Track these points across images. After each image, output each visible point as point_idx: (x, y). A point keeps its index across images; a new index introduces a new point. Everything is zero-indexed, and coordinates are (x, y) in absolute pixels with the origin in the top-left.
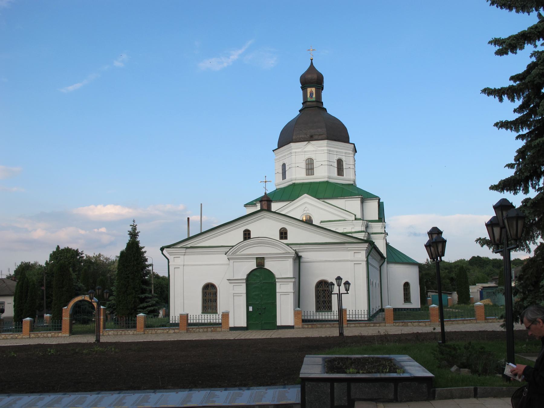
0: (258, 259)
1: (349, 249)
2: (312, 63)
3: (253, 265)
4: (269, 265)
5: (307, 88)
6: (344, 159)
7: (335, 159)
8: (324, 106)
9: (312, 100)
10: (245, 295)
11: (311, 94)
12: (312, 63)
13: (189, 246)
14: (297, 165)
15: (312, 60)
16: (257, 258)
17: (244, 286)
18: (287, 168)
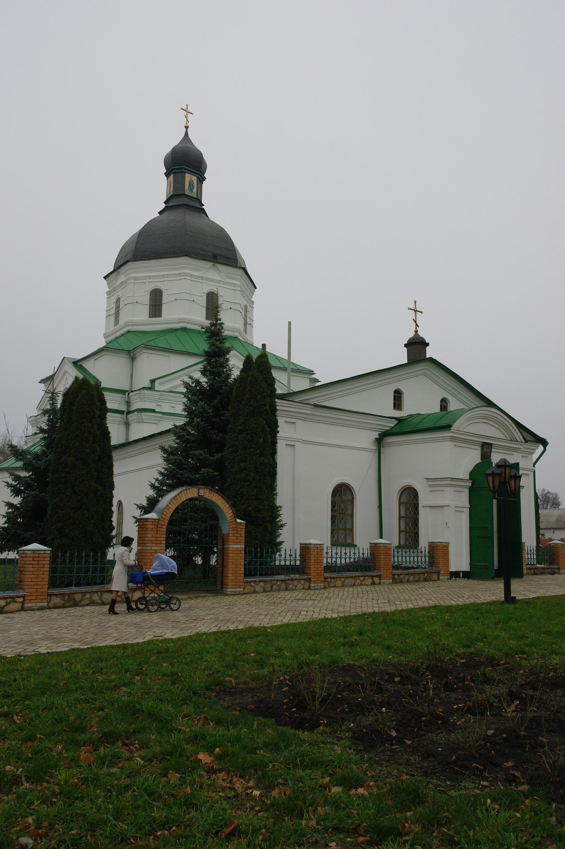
0: (485, 446)
2: (186, 134)
5: (185, 173)
9: (190, 195)
11: (191, 185)
12: (186, 134)
13: (312, 402)
15: (187, 128)
16: (484, 443)
17: (467, 492)
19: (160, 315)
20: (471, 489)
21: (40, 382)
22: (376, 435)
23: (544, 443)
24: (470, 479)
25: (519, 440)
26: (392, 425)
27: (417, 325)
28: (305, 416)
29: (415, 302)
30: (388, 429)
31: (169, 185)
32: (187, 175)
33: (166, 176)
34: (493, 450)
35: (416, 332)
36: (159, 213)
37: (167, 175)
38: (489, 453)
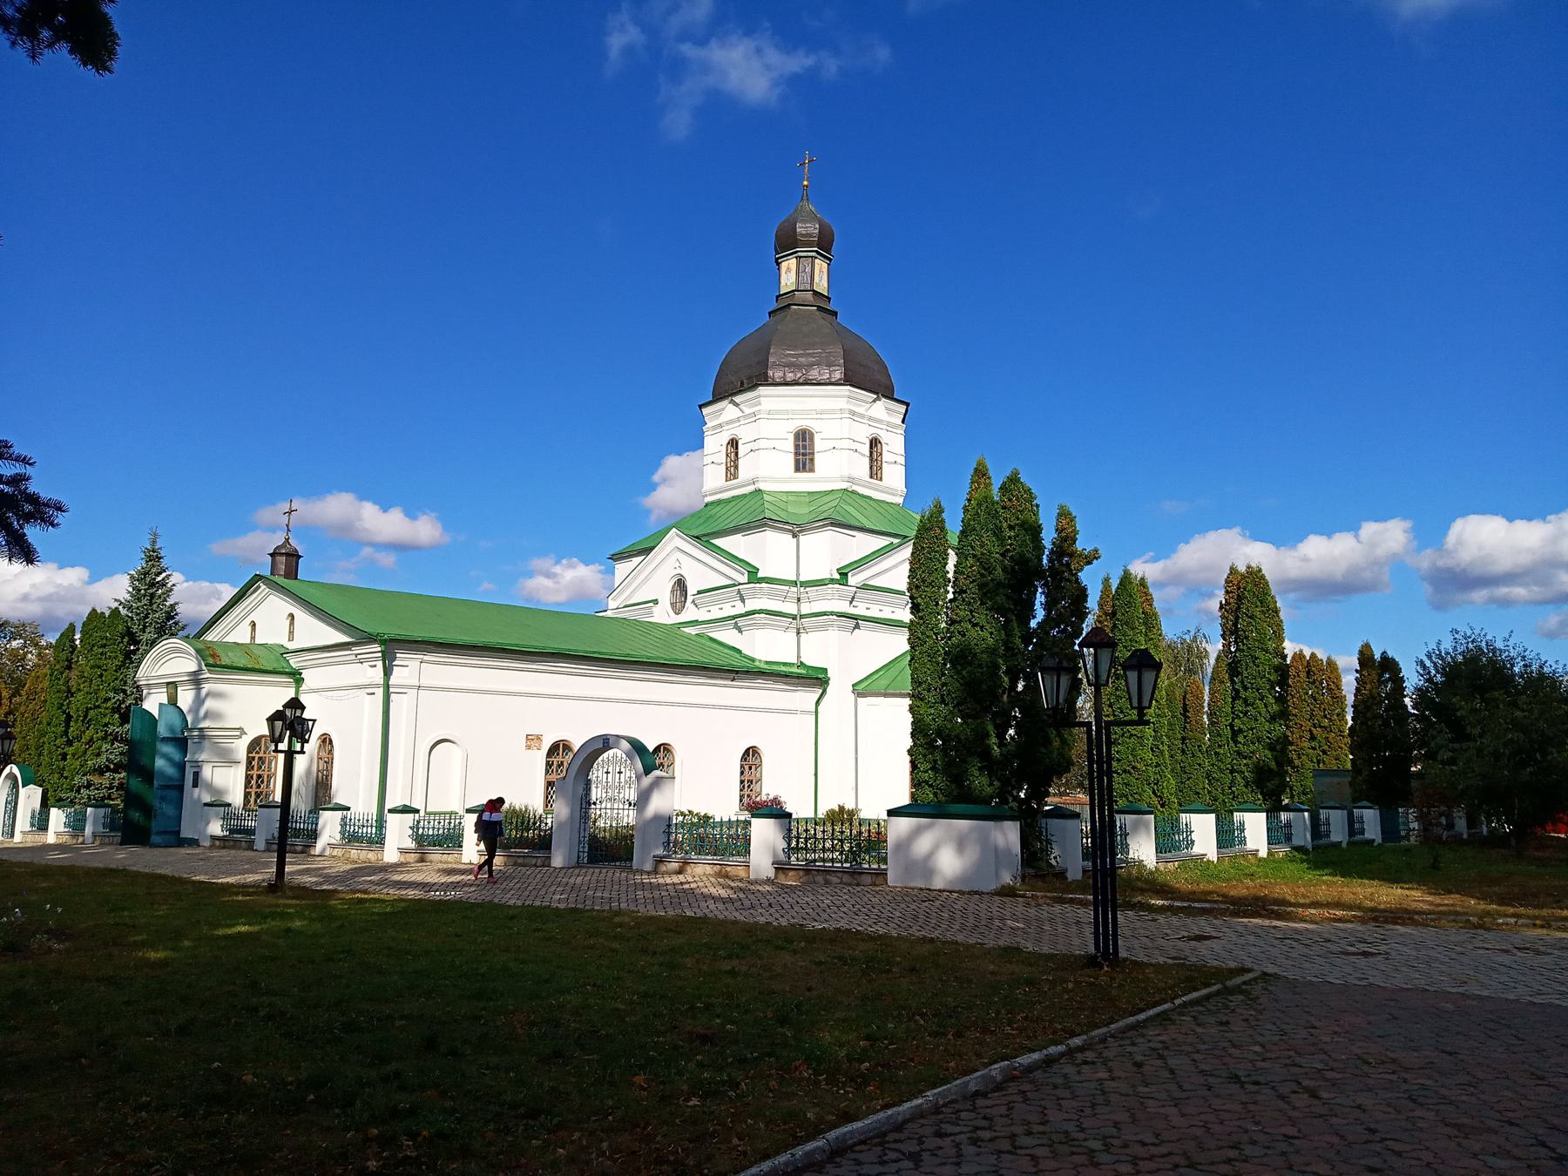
6: (884, 437)
7: (864, 433)
14: (771, 444)
18: (742, 450)
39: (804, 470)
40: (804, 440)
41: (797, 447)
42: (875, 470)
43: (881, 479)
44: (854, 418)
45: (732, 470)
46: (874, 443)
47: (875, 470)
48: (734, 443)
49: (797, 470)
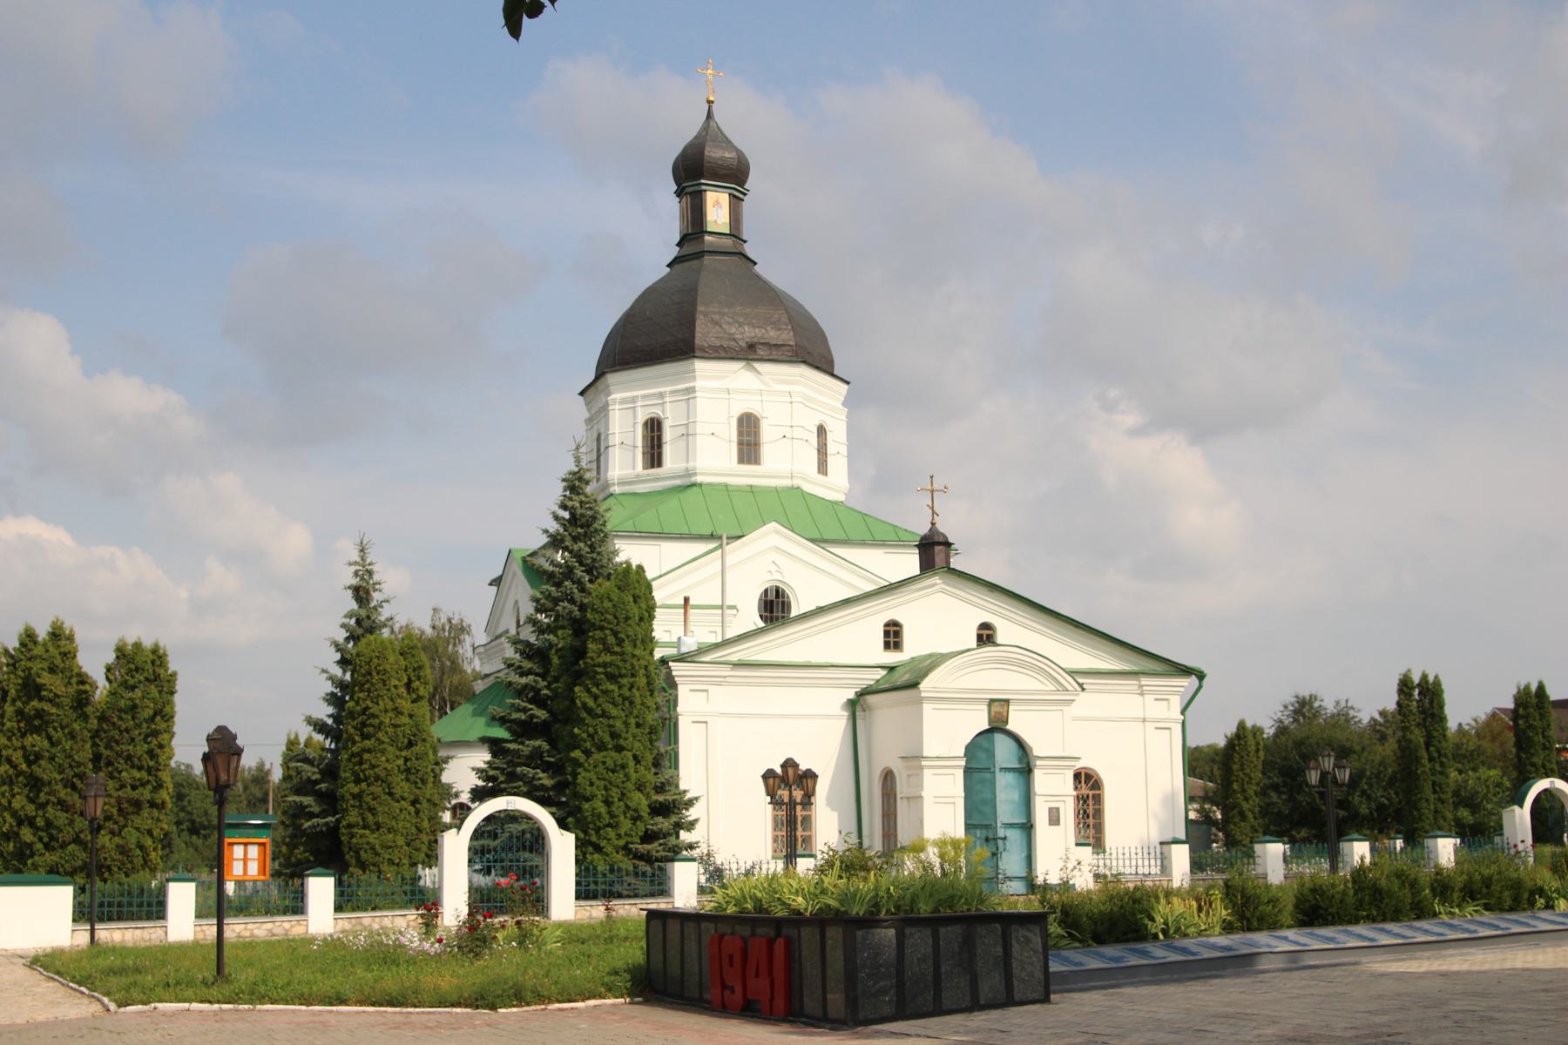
0: (996, 703)
1: (1145, 688)
2: (709, 116)
3: (980, 721)
4: (1018, 722)
5: (705, 191)
8: (749, 250)
10: (963, 800)
12: (709, 116)
13: (734, 658)
16: (992, 701)
17: (960, 774)
18: (668, 434)
19: (660, 465)
20: (968, 771)
21: (491, 584)
22: (851, 694)
23: (1201, 676)
24: (965, 755)
25: (1070, 688)
26: (878, 677)
27: (933, 512)
28: (722, 679)
29: (932, 477)
30: (872, 683)
31: (681, 209)
32: (709, 194)
33: (678, 196)
34: (1011, 707)
35: (933, 524)
36: (668, 266)
37: (679, 193)
38: (1005, 714)
39: (749, 462)
40: (749, 426)
41: (740, 434)
42: (823, 468)
43: (826, 474)
44: (807, 403)
45: (654, 456)
46: (821, 431)
47: (823, 468)
48: (654, 428)
49: (741, 460)
